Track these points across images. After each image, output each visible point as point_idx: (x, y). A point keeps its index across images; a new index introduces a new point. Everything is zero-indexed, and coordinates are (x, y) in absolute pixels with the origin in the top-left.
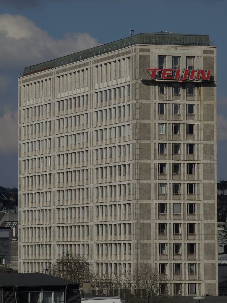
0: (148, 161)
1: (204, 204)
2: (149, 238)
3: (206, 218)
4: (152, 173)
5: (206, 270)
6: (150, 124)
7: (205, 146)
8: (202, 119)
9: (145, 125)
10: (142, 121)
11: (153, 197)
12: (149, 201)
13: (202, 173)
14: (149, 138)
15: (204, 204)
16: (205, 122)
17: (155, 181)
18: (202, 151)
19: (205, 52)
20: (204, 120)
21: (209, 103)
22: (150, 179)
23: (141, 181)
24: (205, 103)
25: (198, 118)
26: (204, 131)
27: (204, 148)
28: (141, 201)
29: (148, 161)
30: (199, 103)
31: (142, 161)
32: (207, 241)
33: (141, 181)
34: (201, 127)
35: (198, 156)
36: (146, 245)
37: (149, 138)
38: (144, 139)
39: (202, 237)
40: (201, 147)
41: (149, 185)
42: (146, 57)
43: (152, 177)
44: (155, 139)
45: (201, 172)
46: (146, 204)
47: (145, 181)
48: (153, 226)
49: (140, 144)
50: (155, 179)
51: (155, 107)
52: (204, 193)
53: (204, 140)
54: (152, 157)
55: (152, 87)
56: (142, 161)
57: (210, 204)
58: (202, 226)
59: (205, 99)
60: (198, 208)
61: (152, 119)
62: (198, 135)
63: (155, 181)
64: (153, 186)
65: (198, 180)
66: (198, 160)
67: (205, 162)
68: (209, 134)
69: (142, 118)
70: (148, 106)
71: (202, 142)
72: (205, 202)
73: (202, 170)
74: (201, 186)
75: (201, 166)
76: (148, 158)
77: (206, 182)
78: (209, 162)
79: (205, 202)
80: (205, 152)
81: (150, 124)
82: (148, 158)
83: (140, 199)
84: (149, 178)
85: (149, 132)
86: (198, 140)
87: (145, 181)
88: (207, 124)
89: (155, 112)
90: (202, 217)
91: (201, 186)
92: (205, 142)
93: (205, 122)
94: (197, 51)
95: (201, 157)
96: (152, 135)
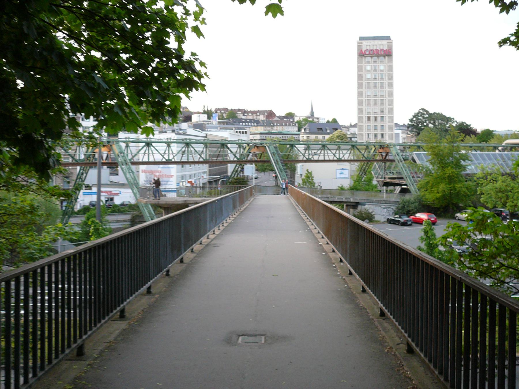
2: (362, 122)
3: (389, 114)
5: (389, 136)
7: (389, 83)
9: (360, 74)
11: (364, 105)
14: (362, 80)
19: (388, 43)
32: (389, 124)
34: (387, 75)
36: (361, 125)
37: (362, 80)
39: (387, 122)
40: (387, 83)
42: (360, 46)
43: (364, 96)
47: (361, 99)
48: (364, 118)
54: (364, 88)
55: (363, 58)
58: (387, 118)
59: (388, 63)
68: (390, 77)
76: (362, 89)
80: (389, 85)
82: (362, 89)
85: (362, 77)
90: (387, 113)
91: (387, 100)
94: (385, 42)
95: (387, 88)
96: (364, 79)
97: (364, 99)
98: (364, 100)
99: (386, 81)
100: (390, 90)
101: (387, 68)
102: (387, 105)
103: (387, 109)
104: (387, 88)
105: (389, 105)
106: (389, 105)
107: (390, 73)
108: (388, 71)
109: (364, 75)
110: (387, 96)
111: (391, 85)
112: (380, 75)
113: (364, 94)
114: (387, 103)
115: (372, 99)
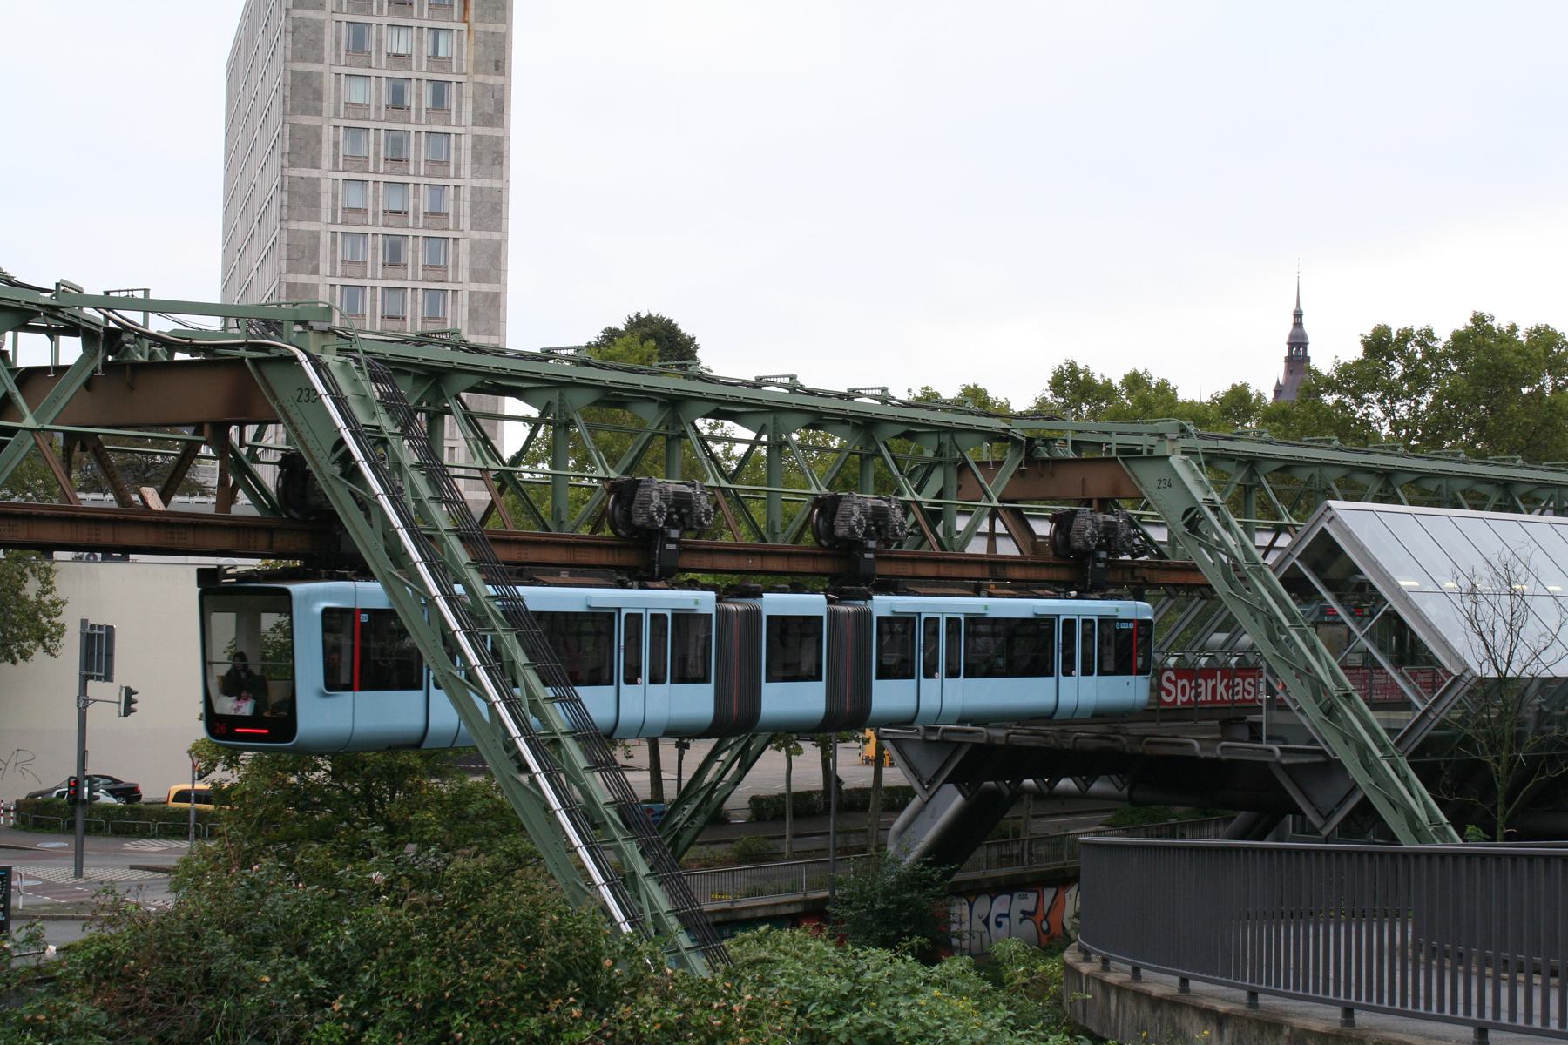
0: (314, 173)
1: (471, 294)
4: (323, 205)
6: (321, 75)
7: (478, 139)
8: (471, 71)
9: (307, 76)
10: (300, 67)
11: (325, 268)
12: (313, 279)
13: (468, 212)
14: (319, 112)
15: (471, 294)
16: (479, 78)
17: (334, 228)
18: (469, 153)
20: (476, 71)
21: (491, 28)
22: (316, 218)
23: (293, 225)
24: (480, 27)
25: (460, 66)
26: (475, 101)
27: (474, 147)
28: (291, 278)
29: (314, 173)
30: (464, 26)
31: (296, 172)
33: (293, 225)
34: (468, 90)
35: (458, 168)
37: (319, 112)
38: (304, 113)
40: (466, 142)
41: (315, 236)
43: (326, 215)
44: (337, 116)
45: (465, 209)
46: (305, 285)
47: (304, 226)
49: (293, 126)
50: (334, 222)
51: (338, 31)
52: (471, 263)
53: (474, 124)
54: (326, 162)
56: (296, 172)
57: (486, 294)
59: (481, 18)
60: (454, 302)
61: (327, 61)
62: (459, 112)
63: (334, 228)
64: (325, 239)
65: (457, 228)
66: (457, 177)
67: (477, 183)
69: (302, 59)
70: (319, 27)
71: (469, 128)
72: (474, 287)
73: (468, 204)
74: (464, 245)
75: (466, 194)
77: (476, 235)
78: (487, 183)
79: (474, 287)
80: (477, 157)
81: (321, 75)
83: (288, 272)
84: (316, 218)
85: (319, 95)
86: (459, 125)
87: (304, 226)
88: (484, 85)
89: (338, 43)
91: (464, 245)
92: (479, 130)
93: (479, 78)
95: (467, 170)
96: (328, 105)
97: (323, 227)
98: (325, 239)
99: (463, 127)
100: (487, 183)
101: (469, 53)
102: (464, 274)
103: (464, 299)
104: (467, 170)
105: (476, 276)
106: (476, 276)
107: (492, 80)
108: (477, 66)
109: (329, 82)
110: (465, 223)
111: (492, 156)
112: (427, 92)
113: (326, 201)
114: (465, 260)
115: (378, 230)
